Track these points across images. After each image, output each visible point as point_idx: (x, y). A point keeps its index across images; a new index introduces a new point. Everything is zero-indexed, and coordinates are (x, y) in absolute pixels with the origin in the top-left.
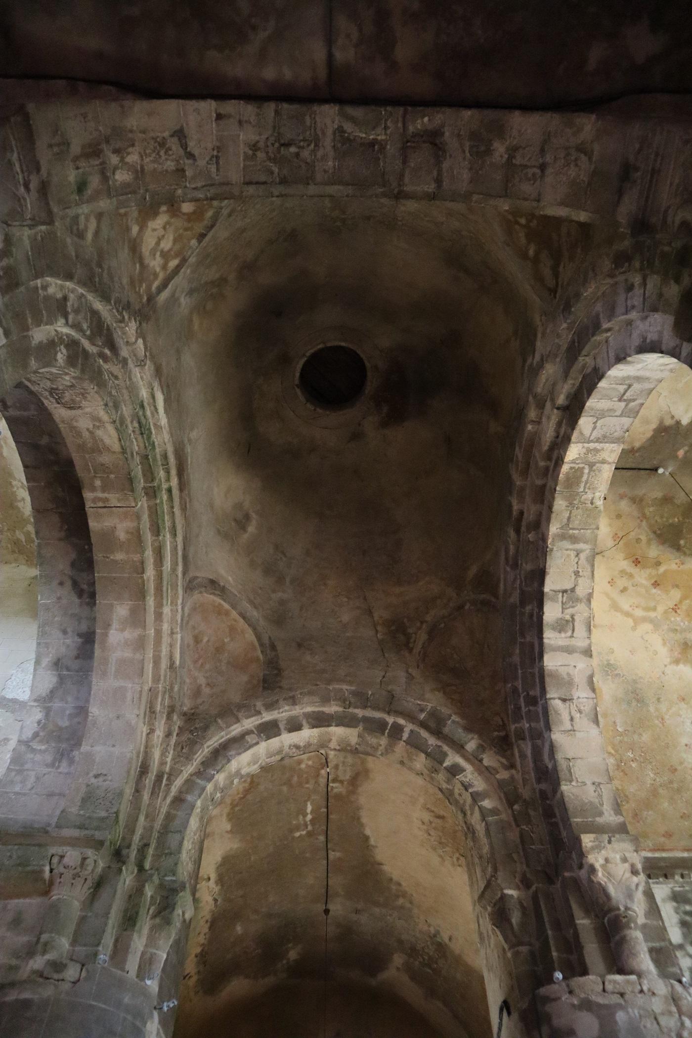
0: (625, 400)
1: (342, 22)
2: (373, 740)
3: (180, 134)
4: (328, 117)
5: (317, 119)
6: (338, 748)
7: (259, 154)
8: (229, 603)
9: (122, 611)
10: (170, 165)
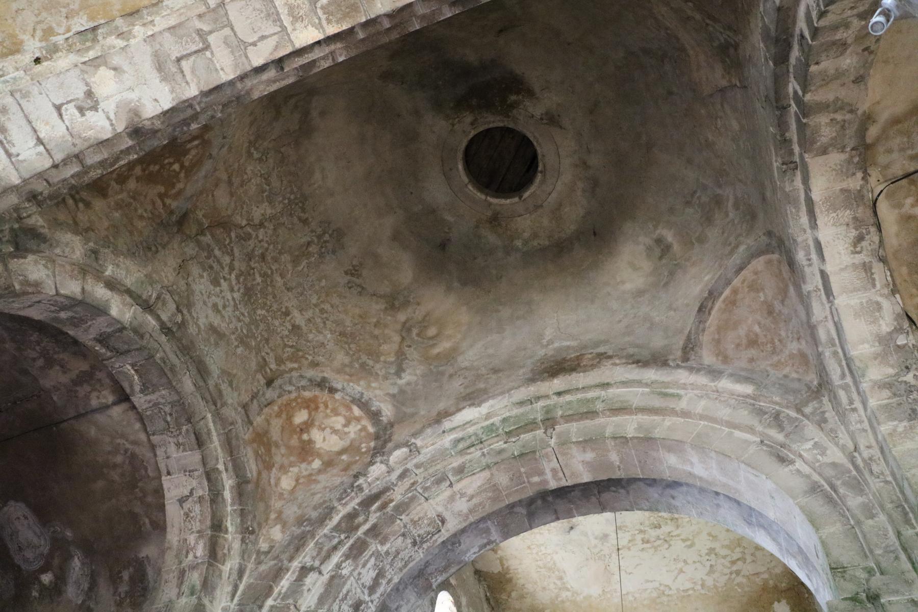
0: (205, 41)
1: (94, 403)
2: (826, 133)
3: (182, 501)
4: (140, 400)
5: (144, 407)
6: (860, 175)
7: (181, 441)
8: (724, 289)
9: (672, 460)
10: (197, 508)
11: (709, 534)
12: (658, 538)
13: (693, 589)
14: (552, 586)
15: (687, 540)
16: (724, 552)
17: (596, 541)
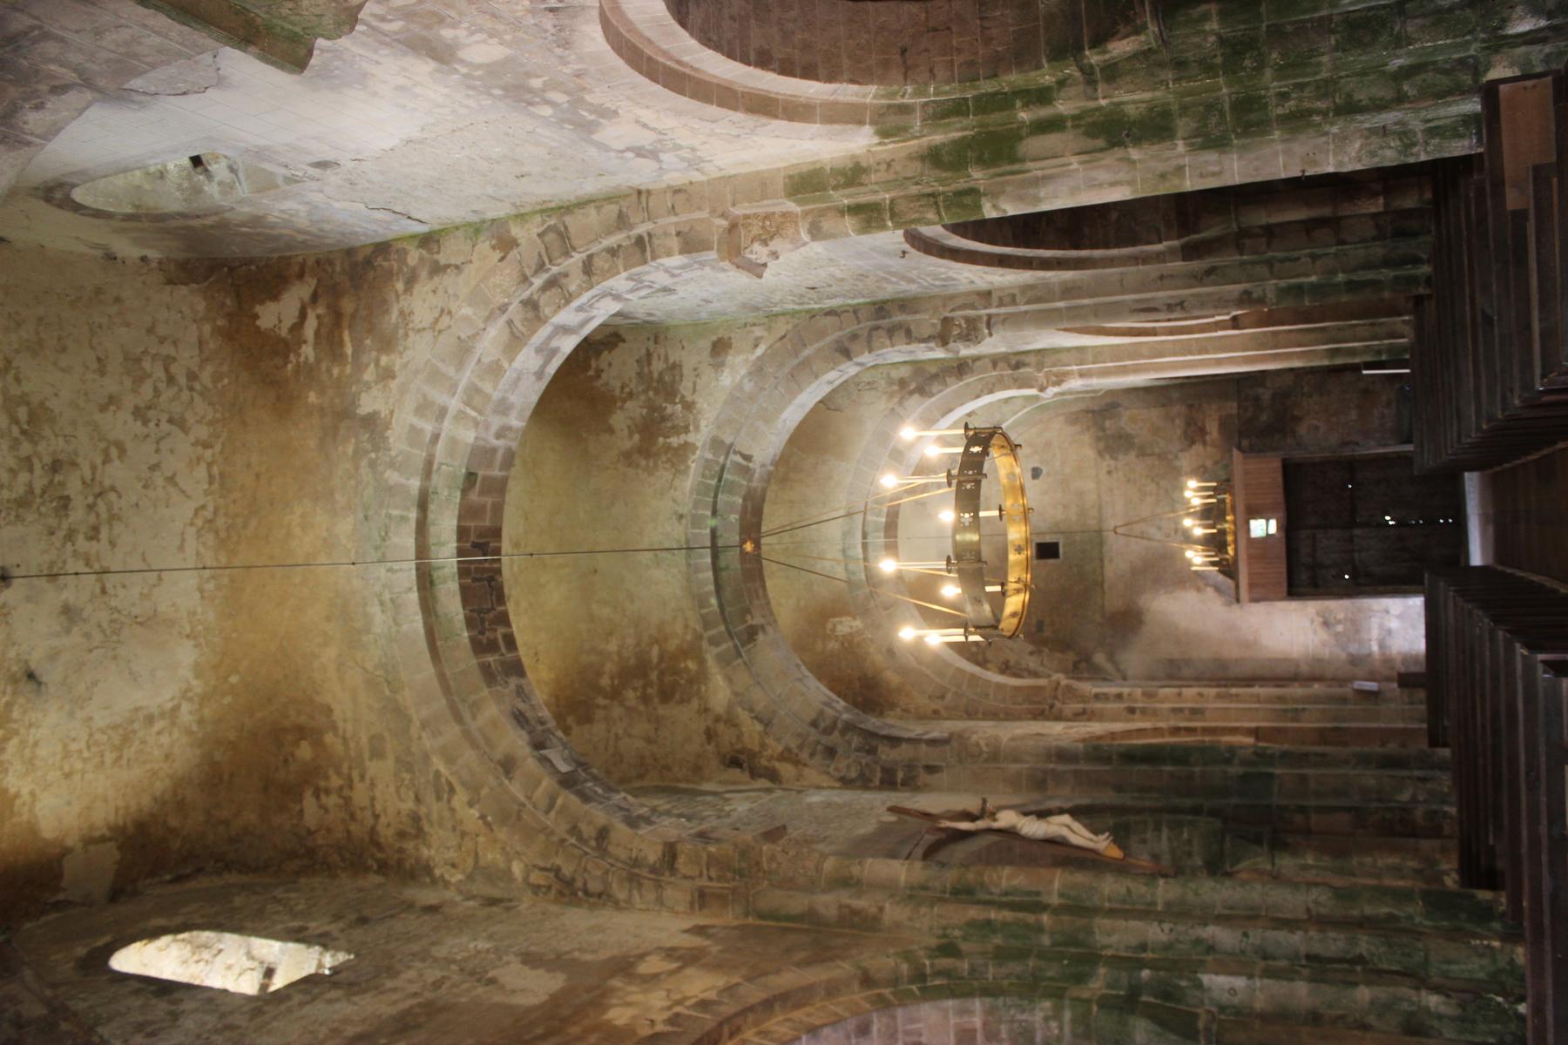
11: (103, 409)
12: (91, 507)
13: (210, 465)
14: (165, 739)
15: (106, 452)
16: (147, 390)
17: (75, 629)
